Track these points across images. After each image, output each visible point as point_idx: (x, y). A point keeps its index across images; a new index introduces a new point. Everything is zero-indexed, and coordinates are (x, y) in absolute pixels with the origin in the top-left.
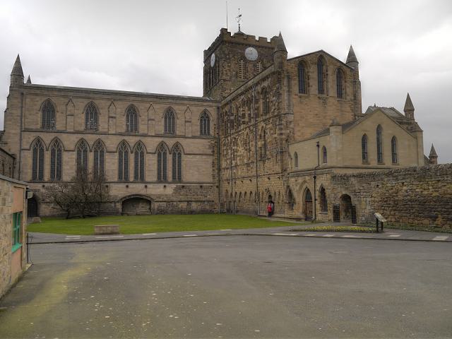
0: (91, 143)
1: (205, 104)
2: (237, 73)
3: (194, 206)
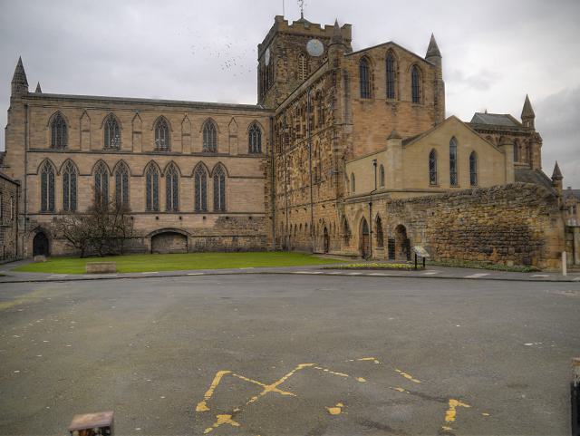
0: (111, 165)
1: (254, 113)
2: (296, 73)
3: (242, 242)
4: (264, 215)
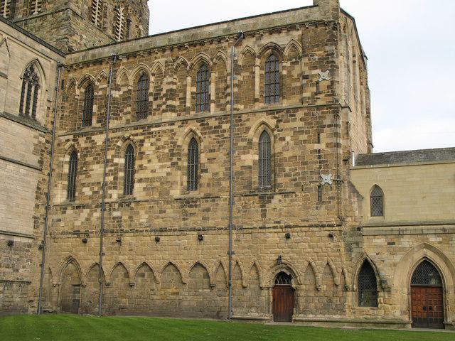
1: (40, 47)
4: (30, 241)
